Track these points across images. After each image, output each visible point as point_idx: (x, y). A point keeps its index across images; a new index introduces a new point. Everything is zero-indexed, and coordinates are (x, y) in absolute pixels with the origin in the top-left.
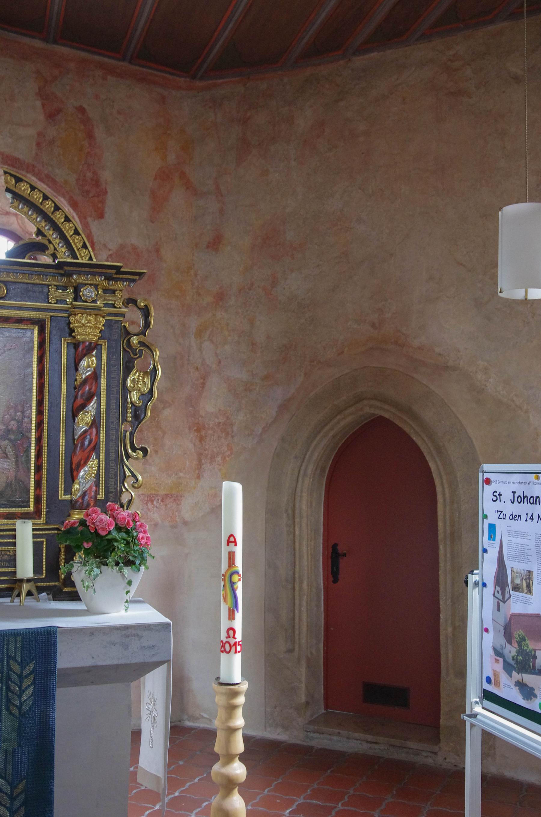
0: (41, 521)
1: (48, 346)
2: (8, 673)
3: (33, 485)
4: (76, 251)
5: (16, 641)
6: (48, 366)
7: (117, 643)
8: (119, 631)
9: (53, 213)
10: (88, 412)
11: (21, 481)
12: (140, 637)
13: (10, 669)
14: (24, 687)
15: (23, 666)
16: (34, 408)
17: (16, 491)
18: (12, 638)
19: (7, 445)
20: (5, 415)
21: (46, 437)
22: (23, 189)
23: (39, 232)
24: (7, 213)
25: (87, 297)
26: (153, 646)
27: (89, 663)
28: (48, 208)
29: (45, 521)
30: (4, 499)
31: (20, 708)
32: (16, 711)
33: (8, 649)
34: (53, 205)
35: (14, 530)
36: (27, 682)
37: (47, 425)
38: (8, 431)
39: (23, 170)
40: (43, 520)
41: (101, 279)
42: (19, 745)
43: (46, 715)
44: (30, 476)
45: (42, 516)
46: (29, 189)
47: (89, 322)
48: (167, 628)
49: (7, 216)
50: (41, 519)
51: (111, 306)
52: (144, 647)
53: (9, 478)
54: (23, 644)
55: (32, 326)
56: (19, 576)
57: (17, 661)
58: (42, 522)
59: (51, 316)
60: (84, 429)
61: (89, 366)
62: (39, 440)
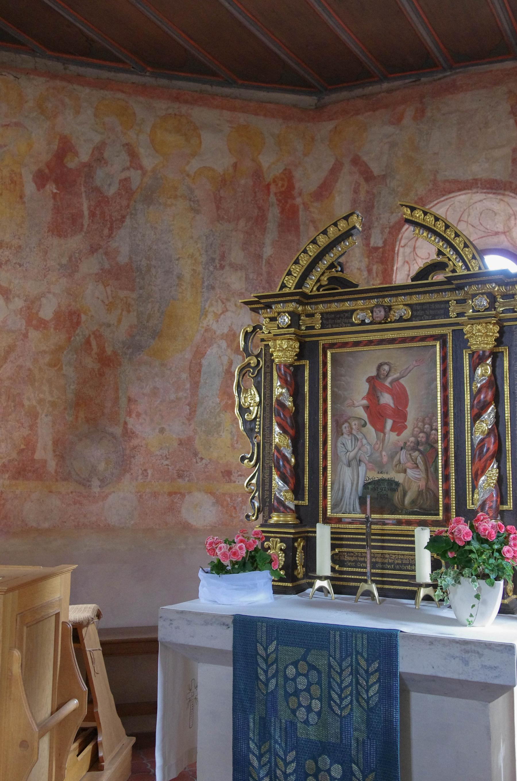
2: (356, 667)
4: (468, 263)
5: (362, 638)
7: (457, 657)
8: (458, 645)
9: (445, 231)
10: (483, 421)
11: (431, 490)
12: (481, 655)
13: (358, 663)
14: (370, 683)
15: (369, 663)
17: (427, 498)
18: (359, 635)
22: (418, 215)
23: (440, 253)
24: (497, 233)
25: (479, 306)
26: (496, 667)
27: (429, 671)
28: (440, 228)
30: (416, 507)
31: (367, 702)
32: (364, 704)
33: (356, 644)
34: (444, 224)
35: (413, 536)
36: (373, 679)
38: (418, 443)
39: (501, 189)
41: (492, 286)
42: (368, 737)
43: (390, 714)
46: (423, 215)
47: (479, 331)
48: (510, 650)
49: (497, 236)
51: (511, 311)
52: (485, 666)
54: (368, 642)
56: (418, 580)
57: (363, 657)
59: (453, 331)
60: (480, 438)
61: (483, 375)
62: (446, 450)
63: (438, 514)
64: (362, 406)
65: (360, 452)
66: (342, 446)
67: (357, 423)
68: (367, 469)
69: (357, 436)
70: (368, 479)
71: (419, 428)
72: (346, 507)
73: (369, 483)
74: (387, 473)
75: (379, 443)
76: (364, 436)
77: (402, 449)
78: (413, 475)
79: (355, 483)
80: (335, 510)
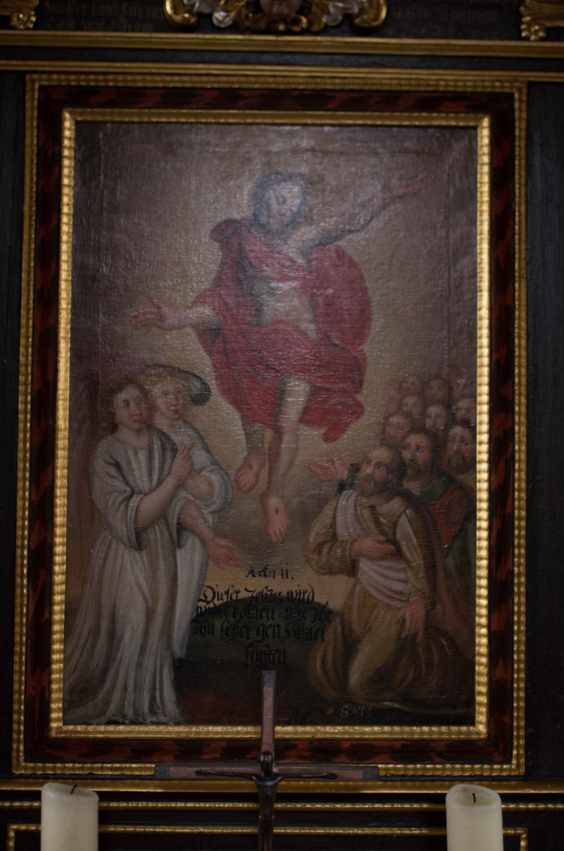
0: (510, 770)
1: (523, 182)
3: (484, 650)
6: (523, 246)
16: (483, 390)
19: (400, 516)
20: (391, 415)
21: (523, 485)
29: (522, 770)
37: (524, 448)
40: (518, 765)
44: (474, 620)
45: (515, 752)
50: (509, 762)
53: (408, 623)
55: (472, 115)
58: (513, 774)
59: (531, 85)
63: (471, 721)
64: (195, 326)
65: (183, 494)
66: (113, 471)
67: (171, 388)
68: (207, 558)
69: (173, 437)
70: (210, 594)
71: (408, 415)
72: (123, 699)
73: (216, 611)
74: (285, 574)
75: (255, 464)
76: (202, 438)
77: (342, 487)
78: (380, 579)
79: (161, 608)
80: (81, 711)
